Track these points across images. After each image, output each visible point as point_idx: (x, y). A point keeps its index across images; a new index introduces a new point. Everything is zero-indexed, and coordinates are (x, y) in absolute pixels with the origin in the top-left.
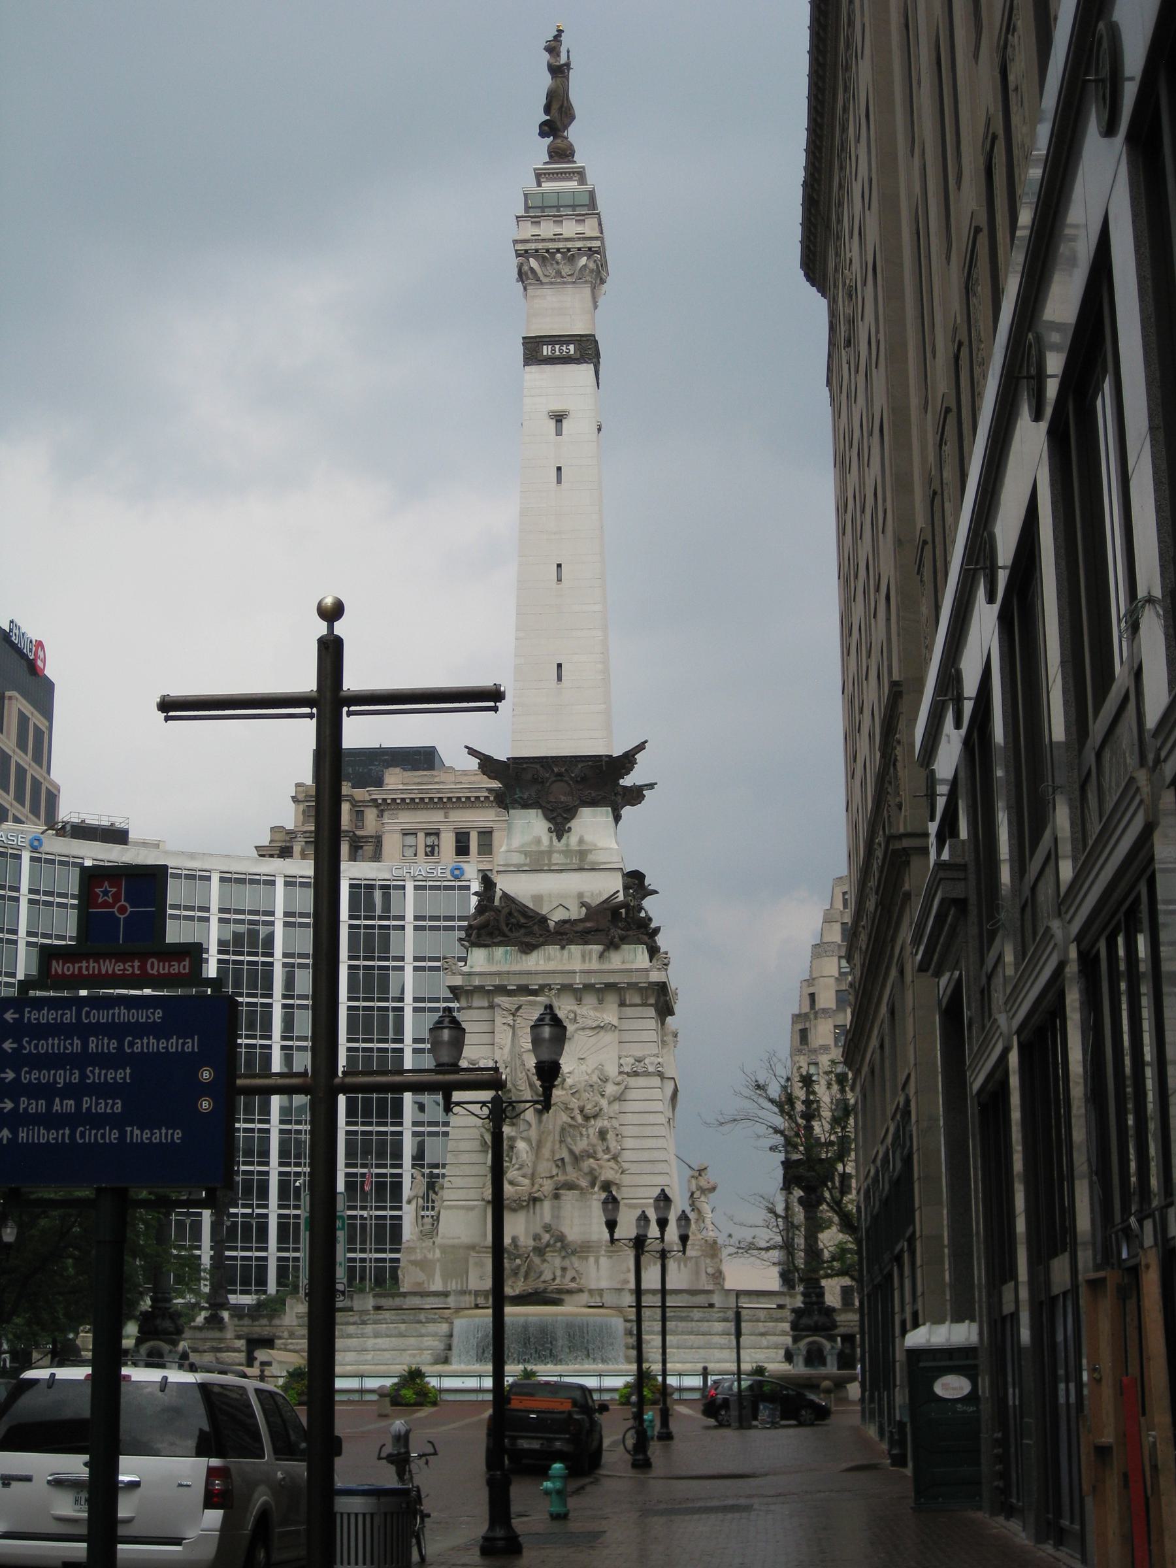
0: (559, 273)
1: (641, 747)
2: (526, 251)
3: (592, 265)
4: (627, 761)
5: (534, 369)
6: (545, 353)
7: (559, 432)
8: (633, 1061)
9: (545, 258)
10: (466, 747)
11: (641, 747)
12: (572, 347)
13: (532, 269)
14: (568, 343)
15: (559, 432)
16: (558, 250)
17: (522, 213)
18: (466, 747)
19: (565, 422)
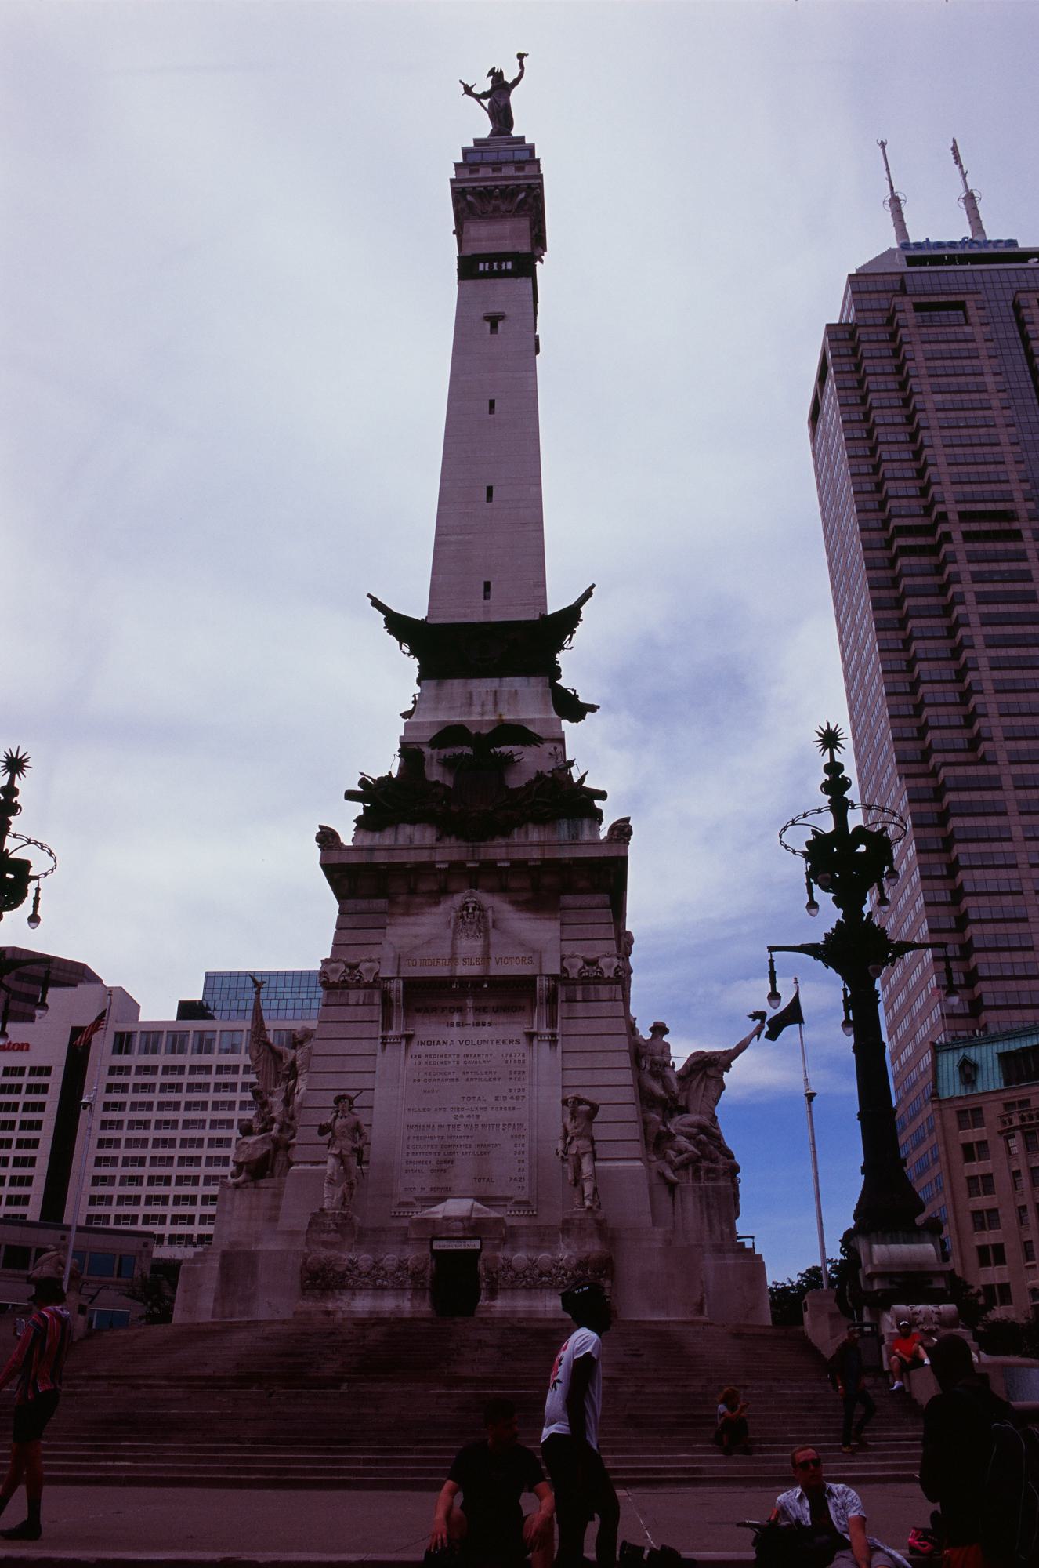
0: (496, 209)
1: (588, 594)
2: (463, 189)
3: (530, 200)
6: (481, 267)
8: (580, 964)
9: (485, 194)
10: (369, 596)
11: (588, 594)
12: (509, 265)
13: (469, 203)
14: (506, 261)
16: (496, 187)
17: (460, 160)
18: (369, 596)
19: (500, 324)
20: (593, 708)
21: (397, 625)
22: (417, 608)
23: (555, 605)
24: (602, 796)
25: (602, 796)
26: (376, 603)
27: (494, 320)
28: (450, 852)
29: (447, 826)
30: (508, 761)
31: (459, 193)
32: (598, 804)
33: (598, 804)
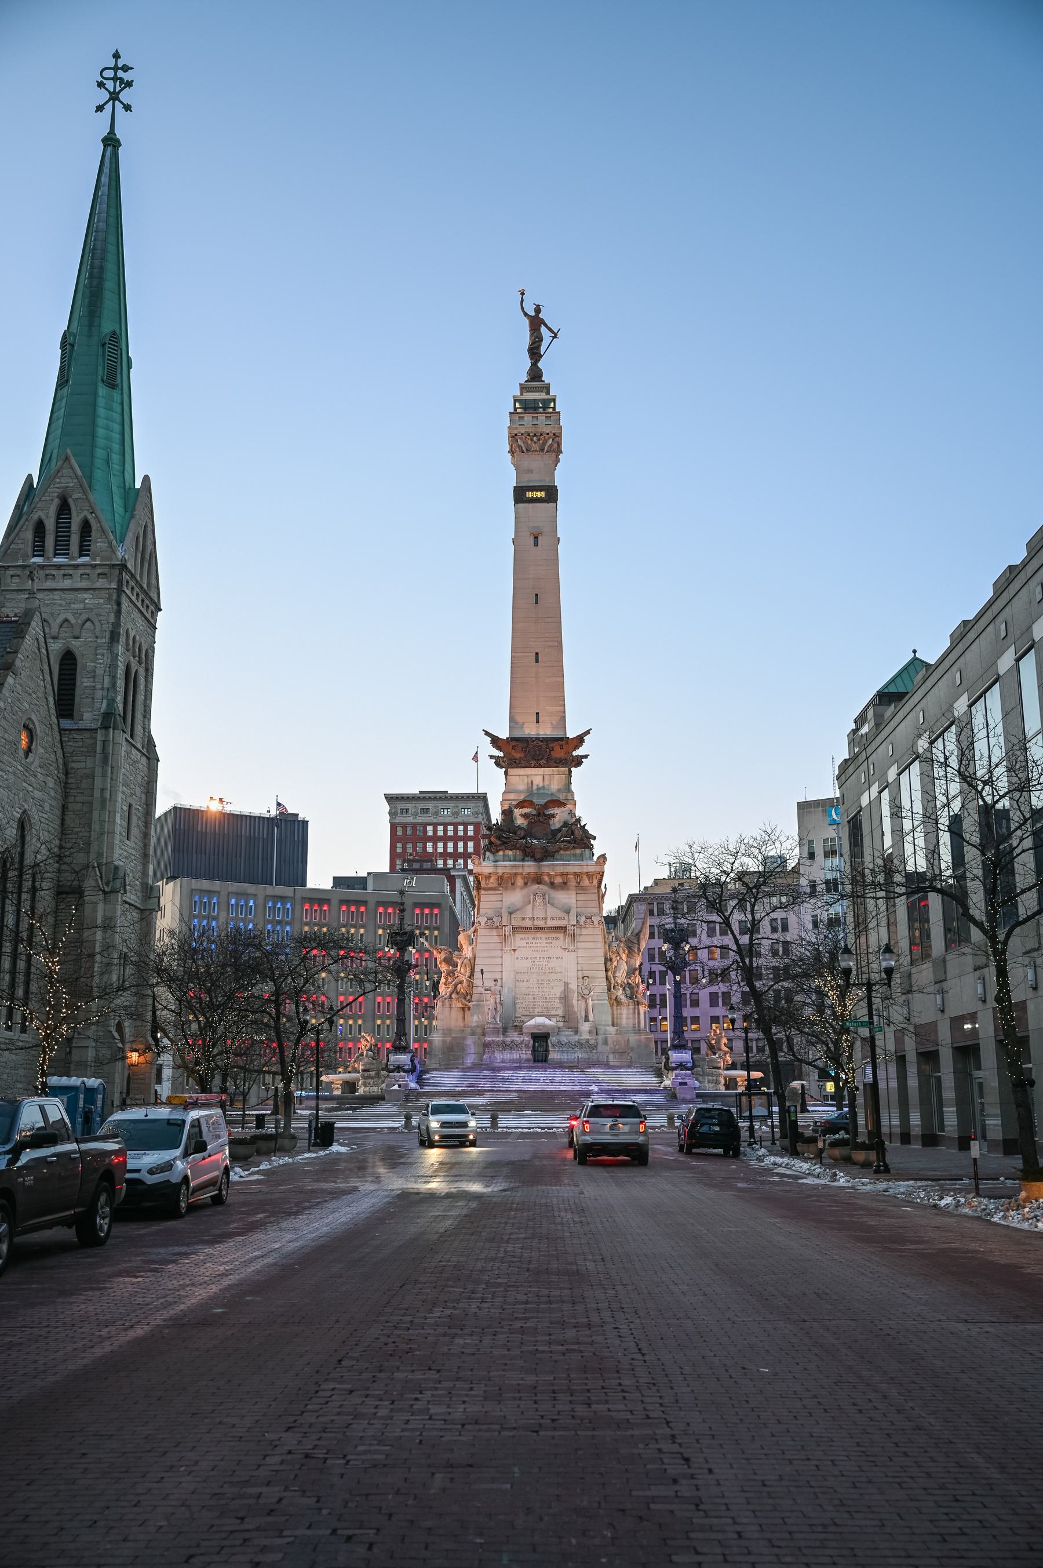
1: (588, 732)
4: (580, 740)
5: (521, 505)
7: (536, 544)
11: (588, 732)
15: (536, 544)
19: (540, 538)
20: (586, 756)
21: (496, 741)
22: (504, 734)
23: (571, 733)
24: (594, 838)
25: (594, 838)
26: (487, 733)
27: (536, 538)
28: (530, 867)
29: (528, 853)
30: (553, 816)
31: (513, 437)
32: (592, 842)
33: (592, 842)
